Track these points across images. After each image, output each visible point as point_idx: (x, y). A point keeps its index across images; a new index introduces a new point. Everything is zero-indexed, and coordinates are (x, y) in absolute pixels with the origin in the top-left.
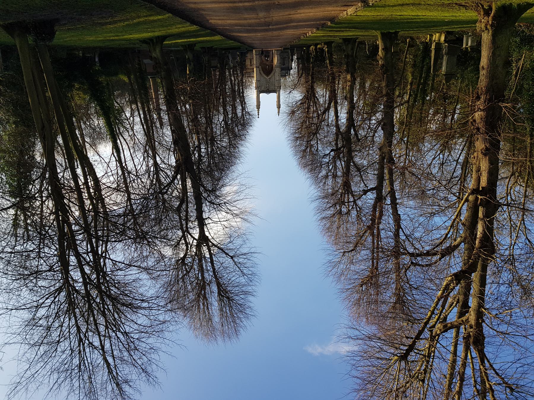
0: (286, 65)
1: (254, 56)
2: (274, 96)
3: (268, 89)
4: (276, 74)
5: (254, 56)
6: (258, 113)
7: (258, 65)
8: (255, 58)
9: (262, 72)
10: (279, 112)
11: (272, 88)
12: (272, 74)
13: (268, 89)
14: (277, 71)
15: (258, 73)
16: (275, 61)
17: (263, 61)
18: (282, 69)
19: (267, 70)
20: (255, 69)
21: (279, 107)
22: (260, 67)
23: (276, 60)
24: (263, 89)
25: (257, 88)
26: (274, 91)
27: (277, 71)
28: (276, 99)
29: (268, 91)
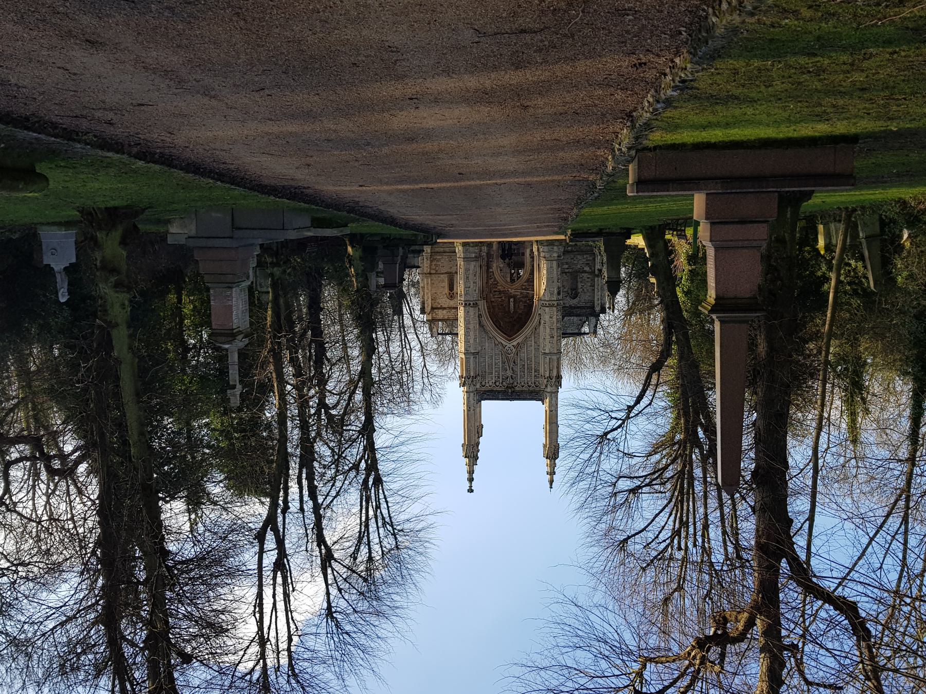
1: (460, 262)
4: (545, 332)
5: (460, 262)
6: (471, 472)
7: (475, 295)
8: (461, 272)
10: (552, 473)
11: (524, 381)
12: (527, 331)
14: (547, 319)
15: (474, 323)
16: (541, 286)
18: (567, 312)
19: (507, 314)
20: (461, 312)
21: (552, 453)
22: (482, 304)
25: (467, 380)
27: (547, 319)
29: (510, 392)
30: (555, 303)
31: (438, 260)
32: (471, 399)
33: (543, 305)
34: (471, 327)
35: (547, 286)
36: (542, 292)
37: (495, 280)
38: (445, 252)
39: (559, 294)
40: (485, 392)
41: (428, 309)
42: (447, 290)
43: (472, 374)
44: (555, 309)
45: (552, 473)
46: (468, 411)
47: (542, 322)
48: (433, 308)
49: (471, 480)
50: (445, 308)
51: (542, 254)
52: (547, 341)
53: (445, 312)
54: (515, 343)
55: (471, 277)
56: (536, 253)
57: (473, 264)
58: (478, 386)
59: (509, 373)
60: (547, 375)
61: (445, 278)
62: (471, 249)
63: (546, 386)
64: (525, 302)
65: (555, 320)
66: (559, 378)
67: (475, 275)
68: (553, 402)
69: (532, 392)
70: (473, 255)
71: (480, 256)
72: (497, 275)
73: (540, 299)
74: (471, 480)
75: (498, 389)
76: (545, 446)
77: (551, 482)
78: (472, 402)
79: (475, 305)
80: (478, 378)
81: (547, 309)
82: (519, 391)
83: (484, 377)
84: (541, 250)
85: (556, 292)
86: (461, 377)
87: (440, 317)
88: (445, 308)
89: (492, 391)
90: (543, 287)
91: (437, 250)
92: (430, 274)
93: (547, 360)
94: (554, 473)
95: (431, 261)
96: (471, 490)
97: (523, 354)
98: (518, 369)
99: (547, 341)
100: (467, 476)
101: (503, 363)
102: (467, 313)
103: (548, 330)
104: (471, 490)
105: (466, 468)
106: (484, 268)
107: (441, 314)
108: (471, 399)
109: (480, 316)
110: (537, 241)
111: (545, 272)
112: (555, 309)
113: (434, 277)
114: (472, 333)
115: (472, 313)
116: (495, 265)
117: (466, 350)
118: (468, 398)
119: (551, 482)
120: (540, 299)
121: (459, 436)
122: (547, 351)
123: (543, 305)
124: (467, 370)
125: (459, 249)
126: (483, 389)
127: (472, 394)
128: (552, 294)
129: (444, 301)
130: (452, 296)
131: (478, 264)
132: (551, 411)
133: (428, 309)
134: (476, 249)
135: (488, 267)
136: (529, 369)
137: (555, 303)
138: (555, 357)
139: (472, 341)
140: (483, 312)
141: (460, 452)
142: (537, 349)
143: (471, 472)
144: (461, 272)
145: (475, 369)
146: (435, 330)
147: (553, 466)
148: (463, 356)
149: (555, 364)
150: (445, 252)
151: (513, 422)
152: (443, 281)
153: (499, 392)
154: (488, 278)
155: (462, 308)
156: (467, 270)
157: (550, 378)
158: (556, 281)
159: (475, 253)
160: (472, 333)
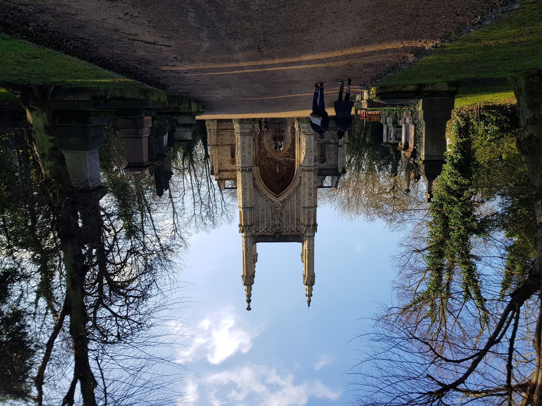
0: (330, 162)
1: (238, 137)
2: (295, 249)
3: (278, 233)
4: (304, 191)
5: (238, 137)
6: (249, 296)
7: (249, 163)
9: (261, 185)
11: (289, 227)
12: (290, 190)
13: (278, 233)
16: (301, 155)
17: (266, 152)
22: (256, 170)
23: (304, 151)
24: (262, 229)
25: (245, 228)
26: (296, 237)
28: (301, 268)
29: (278, 236)
30: (313, 168)
31: (223, 135)
32: (248, 242)
33: (303, 170)
34: (247, 187)
35: (306, 155)
36: (302, 159)
37: (265, 150)
38: (227, 129)
39: (315, 161)
40: (259, 236)
41: (216, 171)
42: (229, 158)
43: (249, 224)
44: (312, 173)
45: (310, 295)
46: (246, 251)
47: (302, 183)
48: (220, 171)
49: (249, 301)
50: (228, 171)
51: (302, 130)
52: (306, 198)
53: (229, 173)
54: (281, 200)
55: (246, 148)
56: (297, 129)
57: (248, 138)
58: (253, 232)
59: (277, 222)
60: (306, 223)
61: (228, 148)
62: (246, 126)
63: (306, 232)
64: (288, 166)
65: (312, 181)
66: (315, 225)
67: (250, 147)
68: (311, 243)
69: (294, 236)
70: (248, 131)
71: (253, 131)
72: (267, 146)
73: (300, 165)
74: (249, 301)
75: (269, 234)
76: (304, 276)
77: (309, 302)
78: (249, 244)
79: (250, 170)
80: (254, 226)
81: (306, 173)
82: (284, 236)
83: (258, 225)
84: (301, 126)
85: (313, 160)
86: (240, 225)
87: (225, 177)
88: (228, 171)
89: (264, 236)
90: (303, 156)
91: (222, 127)
92: (217, 145)
93: (306, 212)
94: (311, 295)
95: (218, 136)
96: (249, 309)
97: (288, 208)
98: (284, 219)
99: (306, 198)
100: (246, 298)
101: (273, 214)
102: (244, 177)
103: (307, 190)
104: (249, 309)
105: (245, 293)
106: (257, 141)
107: (225, 175)
108: (248, 242)
109: (254, 179)
110: (298, 119)
111: (304, 144)
112: (312, 173)
113: (221, 148)
114: (248, 193)
115: (247, 177)
116: (265, 139)
117: (243, 205)
118: (246, 242)
119: (309, 302)
120: (300, 165)
121: (240, 270)
122: (306, 206)
123: (303, 170)
124: (244, 220)
125: (236, 126)
126: (257, 234)
127: (249, 239)
128: (310, 161)
129: (228, 166)
130: (233, 162)
131: (252, 138)
132: (309, 250)
133: (216, 171)
134: (250, 126)
135: (260, 140)
136: (293, 219)
137: (313, 168)
138: (312, 210)
139: (248, 198)
140: (256, 176)
141: (241, 282)
142: (298, 204)
143: (249, 296)
144: (239, 144)
145: (251, 219)
146: (222, 186)
147: (310, 290)
148: (242, 210)
149: (313, 215)
150: (227, 129)
151: (279, 258)
152: (227, 151)
153: (269, 236)
154: (260, 148)
155: (240, 173)
156: (243, 143)
157: (309, 225)
158: (313, 151)
159: (249, 128)
160: (248, 193)
